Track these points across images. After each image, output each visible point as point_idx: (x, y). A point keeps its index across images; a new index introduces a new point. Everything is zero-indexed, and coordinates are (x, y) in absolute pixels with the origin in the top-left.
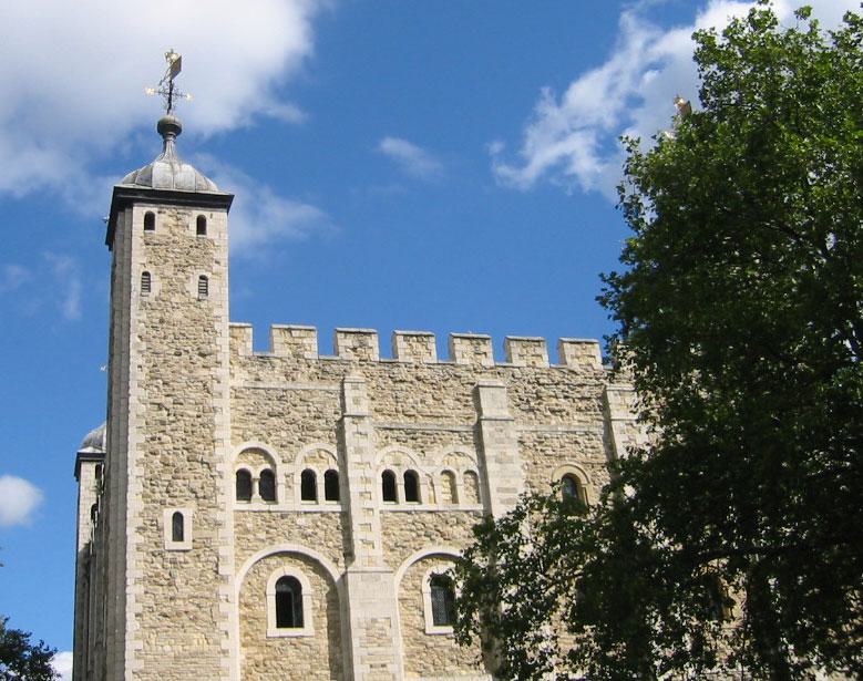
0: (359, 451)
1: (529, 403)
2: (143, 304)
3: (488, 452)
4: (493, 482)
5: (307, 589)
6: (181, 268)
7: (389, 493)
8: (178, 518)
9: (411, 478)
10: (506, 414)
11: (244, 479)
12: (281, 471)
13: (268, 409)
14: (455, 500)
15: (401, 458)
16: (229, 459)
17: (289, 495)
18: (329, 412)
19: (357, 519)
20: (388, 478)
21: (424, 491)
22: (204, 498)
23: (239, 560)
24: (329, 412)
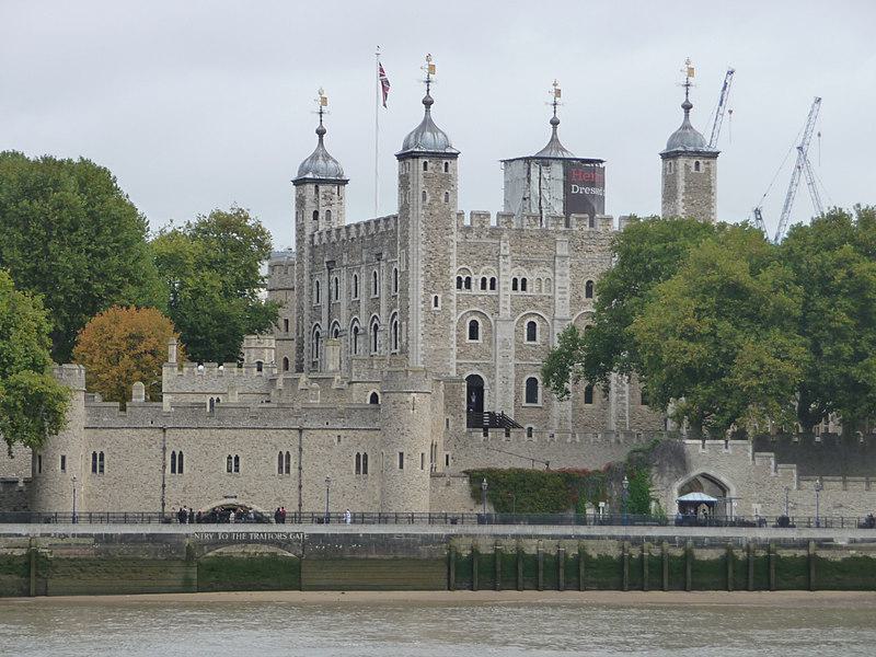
0: (504, 270)
1: (576, 248)
2: (423, 207)
3: (557, 271)
4: (558, 284)
5: (480, 325)
6: (438, 189)
7: (515, 288)
8: (436, 298)
9: (524, 280)
10: (567, 253)
11: (459, 279)
12: (473, 278)
13: (467, 251)
14: (540, 290)
15: (523, 273)
16: (454, 273)
17: (476, 289)
18: (494, 252)
19: (502, 299)
20: (515, 280)
21: (528, 287)
22: (446, 289)
23: (458, 314)
24: (494, 252)
